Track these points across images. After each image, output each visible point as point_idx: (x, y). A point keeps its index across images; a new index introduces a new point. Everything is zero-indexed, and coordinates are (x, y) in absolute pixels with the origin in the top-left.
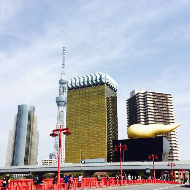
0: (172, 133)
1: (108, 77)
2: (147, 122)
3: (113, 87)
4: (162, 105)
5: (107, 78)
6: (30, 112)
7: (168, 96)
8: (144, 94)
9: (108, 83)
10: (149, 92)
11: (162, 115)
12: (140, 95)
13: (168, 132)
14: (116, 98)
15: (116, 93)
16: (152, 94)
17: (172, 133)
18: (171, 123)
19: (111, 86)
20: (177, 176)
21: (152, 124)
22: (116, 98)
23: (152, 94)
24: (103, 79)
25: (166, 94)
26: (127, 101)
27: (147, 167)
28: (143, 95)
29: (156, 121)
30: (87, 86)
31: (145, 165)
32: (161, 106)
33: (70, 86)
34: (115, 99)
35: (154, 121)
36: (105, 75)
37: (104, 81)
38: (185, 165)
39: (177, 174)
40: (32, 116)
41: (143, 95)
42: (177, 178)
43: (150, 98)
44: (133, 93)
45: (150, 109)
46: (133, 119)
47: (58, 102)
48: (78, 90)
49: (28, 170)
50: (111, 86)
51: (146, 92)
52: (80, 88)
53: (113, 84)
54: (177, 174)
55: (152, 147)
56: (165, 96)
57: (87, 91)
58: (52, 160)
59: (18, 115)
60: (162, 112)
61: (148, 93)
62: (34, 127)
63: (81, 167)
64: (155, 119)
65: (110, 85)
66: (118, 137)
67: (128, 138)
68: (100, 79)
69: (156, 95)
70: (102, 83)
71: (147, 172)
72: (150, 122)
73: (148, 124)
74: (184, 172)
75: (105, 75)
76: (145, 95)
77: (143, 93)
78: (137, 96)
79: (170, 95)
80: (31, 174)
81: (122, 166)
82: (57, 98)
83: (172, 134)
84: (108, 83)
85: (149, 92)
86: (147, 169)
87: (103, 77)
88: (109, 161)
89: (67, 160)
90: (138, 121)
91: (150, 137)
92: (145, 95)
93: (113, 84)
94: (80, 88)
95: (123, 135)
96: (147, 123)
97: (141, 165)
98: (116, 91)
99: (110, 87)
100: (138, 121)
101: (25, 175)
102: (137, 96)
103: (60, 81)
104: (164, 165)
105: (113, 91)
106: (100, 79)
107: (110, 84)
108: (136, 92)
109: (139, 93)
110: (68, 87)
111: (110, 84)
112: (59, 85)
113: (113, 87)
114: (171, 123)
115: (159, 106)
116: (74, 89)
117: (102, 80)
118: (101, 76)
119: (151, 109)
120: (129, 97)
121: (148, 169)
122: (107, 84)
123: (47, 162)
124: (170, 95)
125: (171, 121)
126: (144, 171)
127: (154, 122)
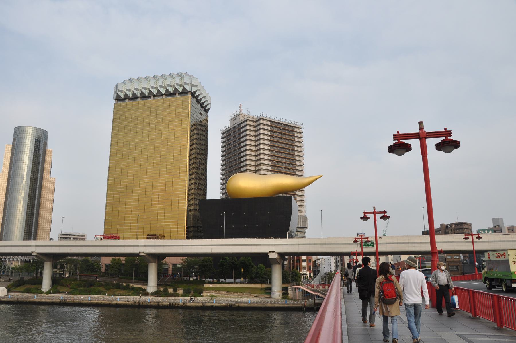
3: (204, 102)
7: (296, 130)
8: (256, 122)
9: (195, 92)
12: (248, 123)
15: (208, 114)
16: (269, 123)
17: (298, 193)
19: (201, 100)
22: (206, 127)
23: (269, 123)
24: (186, 84)
25: (292, 126)
27: (272, 249)
28: (254, 124)
35: (271, 171)
37: (188, 88)
39: (304, 261)
41: (254, 124)
42: (304, 269)
43: (266, 130)
46: (232, 165)
48: (135, 102)
50: (201, 100)
51: (260, 119)
52: (139, 99)
53: (204, 97)
54: (304, 261)
55: (273, 214)
56: (290, 129)
61: (261, 122)
66: (206, 195)
69: (276, 125)
70: (185, 92)
74: (314, 258)
78: (242, 125)
84: (195, 92)
86: (270, 252)
88: (188, 238)
90: (242, 169)
93: (204, 97)
94: (139, 99)
98: (207, 111)
101: (24, 258)
104: (304, 245)
105: (202, 110)
107: (198, 96)
110: (118, 96)
111: (198, 96)
113: (204, 102)
116: (127, 100)
122: (193, 94)
125: (297, 173)
126: (265, 255)
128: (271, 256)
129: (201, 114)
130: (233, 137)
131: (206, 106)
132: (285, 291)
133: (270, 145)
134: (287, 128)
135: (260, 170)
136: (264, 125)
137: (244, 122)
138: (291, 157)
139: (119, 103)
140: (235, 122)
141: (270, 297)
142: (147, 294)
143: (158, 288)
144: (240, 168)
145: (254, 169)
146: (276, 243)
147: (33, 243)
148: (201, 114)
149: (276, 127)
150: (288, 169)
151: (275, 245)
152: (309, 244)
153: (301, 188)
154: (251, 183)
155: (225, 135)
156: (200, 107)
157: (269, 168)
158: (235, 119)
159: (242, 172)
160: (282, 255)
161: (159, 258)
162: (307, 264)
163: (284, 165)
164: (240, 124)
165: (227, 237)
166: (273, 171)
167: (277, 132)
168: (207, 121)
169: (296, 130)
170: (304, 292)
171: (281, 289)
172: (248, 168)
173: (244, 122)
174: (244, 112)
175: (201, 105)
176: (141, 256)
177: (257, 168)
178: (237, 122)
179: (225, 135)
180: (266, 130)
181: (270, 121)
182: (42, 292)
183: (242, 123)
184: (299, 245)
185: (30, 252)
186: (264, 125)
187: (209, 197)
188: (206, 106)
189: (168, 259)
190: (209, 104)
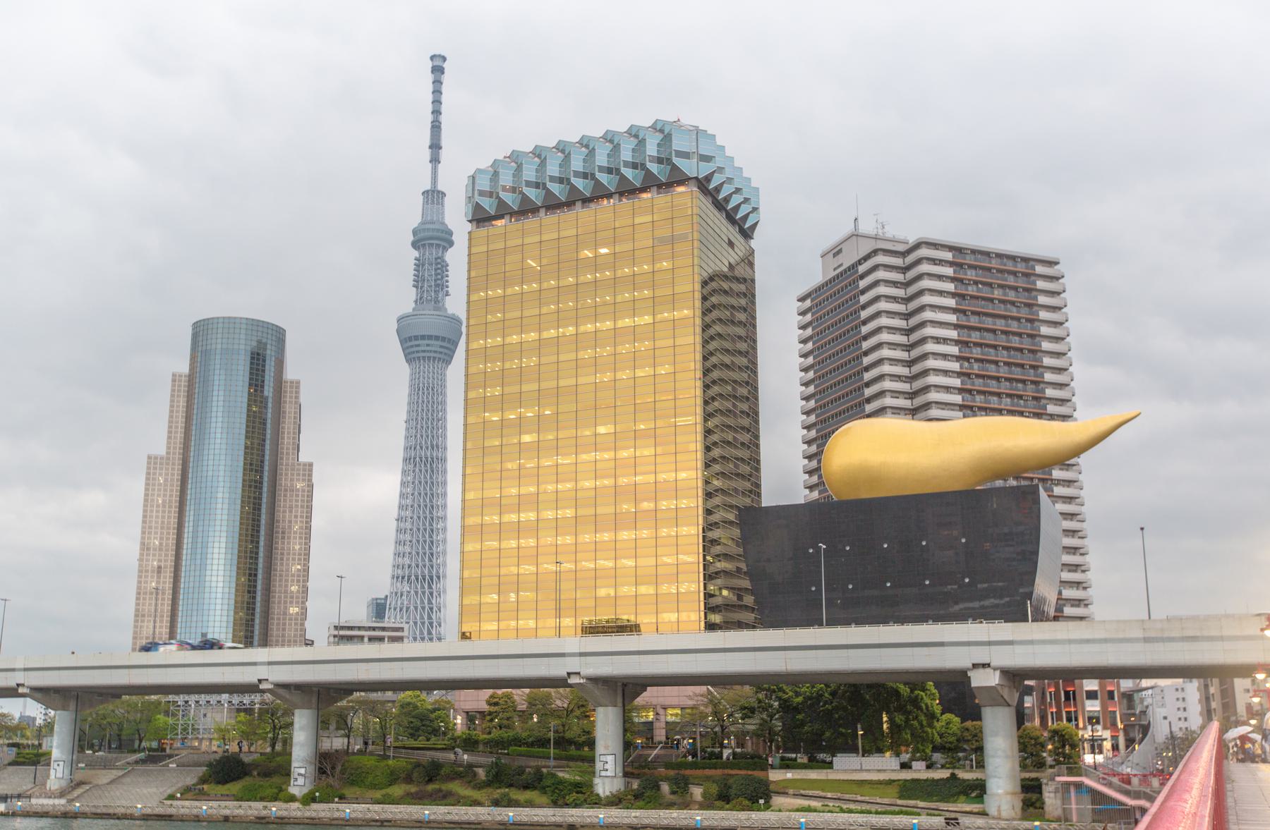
0: (1057, 474)
2: (918, 408)
3: (737, 208)
4: (1000, 321)
7: (1039, 269)
8: (904, 254)
9: (708, 178)
11: (1003, 372)
12: (881, 259)
13: (1026, 471)
15: (753, 243)
16: (948, 256)
17: (1057, 474)
19: (727, 200)
20: (1093, 706)
22: (749, 282)
23: (948, 256)
25: (1026, 260)
26: (802, 299)
27: (980, 655)
28: (898, 261)
29: (971, 408)
32: (1000, 324)
35: (962, 407)
39: (1092, 695)
41: (898, 261)
42: (1093, 720)
44: (840, 251)
45: (938, 340)
47: (410, 339)
48: (530, 222)
50: (727, 200)
51: (917, 246)
52: (542, 211)
53: (738, 190)
54: (1092, 695)
56: (1021, 267)
58: (383, 629)
59: (191, 377)
60: (1003, 356)
61: (924, 252)
62: (286, 440)
63: (563, 655)
64: (967, 396)
65: (721, 197)
66: (759, 495)
69: (969, 260)
71: (974, 684)
74: (1126, 684)
77: (901, 248)
78: (862, 269)
79: (1052, 263)
80: (268, 697)
84: (708, 178)
86: (975, 666)
90: (869, 408)
91: (957, 487)
93: (738, 190)
94: (542, 211)
97: (942, 644)
98: (747, 234)
101: (236, 699)
102: (862, 269)
104: (1088, 641)
107: (718, 189)
110: (478, 208)
111: (718, 189)
112: (416, 254)
113: (737, 208)
115: (989, 323)
117: (676, 160)
119: (945, 341)
120: (816, 276)
121: (985, 666)
122: (702, 184)
123: (362, 637)
125: (1051, 409)
128: (980, 680)
129: (731, 244)
130: (836, 309)
131: (746, 217)
132: (1031, 794)
133: (956, 327)
134: (1010, 266)
135: (927, 406)
137: (866, 258)
138: (1027, 360)
139: (483, 232)
140: (840, 259)
141: (984, 814)
142: (597, 802)
143: (627, 784)
144: (861, 404)
145: (906, 403)
146: (993, 638)
147: (259, 654)
148: (731, 244)
149: (971, 267)
150: (1020, 397)
151: (990, 643)
152: (1105, 641)
153: (1066, 458)
154: (897, 448)
155: (808, 303)
156: (725, 222)
157: (957, 399)
158: (837, 251)
159: (869, 416)
160: (1014, 676)
161: (626, 690)
162: (1104, 706)
163: (1005, 387)
164: (854, 267)
165: (832, 622)
166: (968, 410)
167: (976, 283)
168: (751, 265)
169: (1039, 269)
170: (1097, 797)
171: (1019, 789)
172: (888, 401)
173: (866, 258)
174: (867, 227)
175: (730, 218)
176: (570, 686)
177: (919, 401)
178: (847, 260)
179: (808, 303)
180: (940, 277)
181: (951, 248)
182: (292, 799)
183: (860, 262)
185: (255, 680)
187: (768, 499)
188: (746, 217)
189: (651, 695)
190: (755, 209)
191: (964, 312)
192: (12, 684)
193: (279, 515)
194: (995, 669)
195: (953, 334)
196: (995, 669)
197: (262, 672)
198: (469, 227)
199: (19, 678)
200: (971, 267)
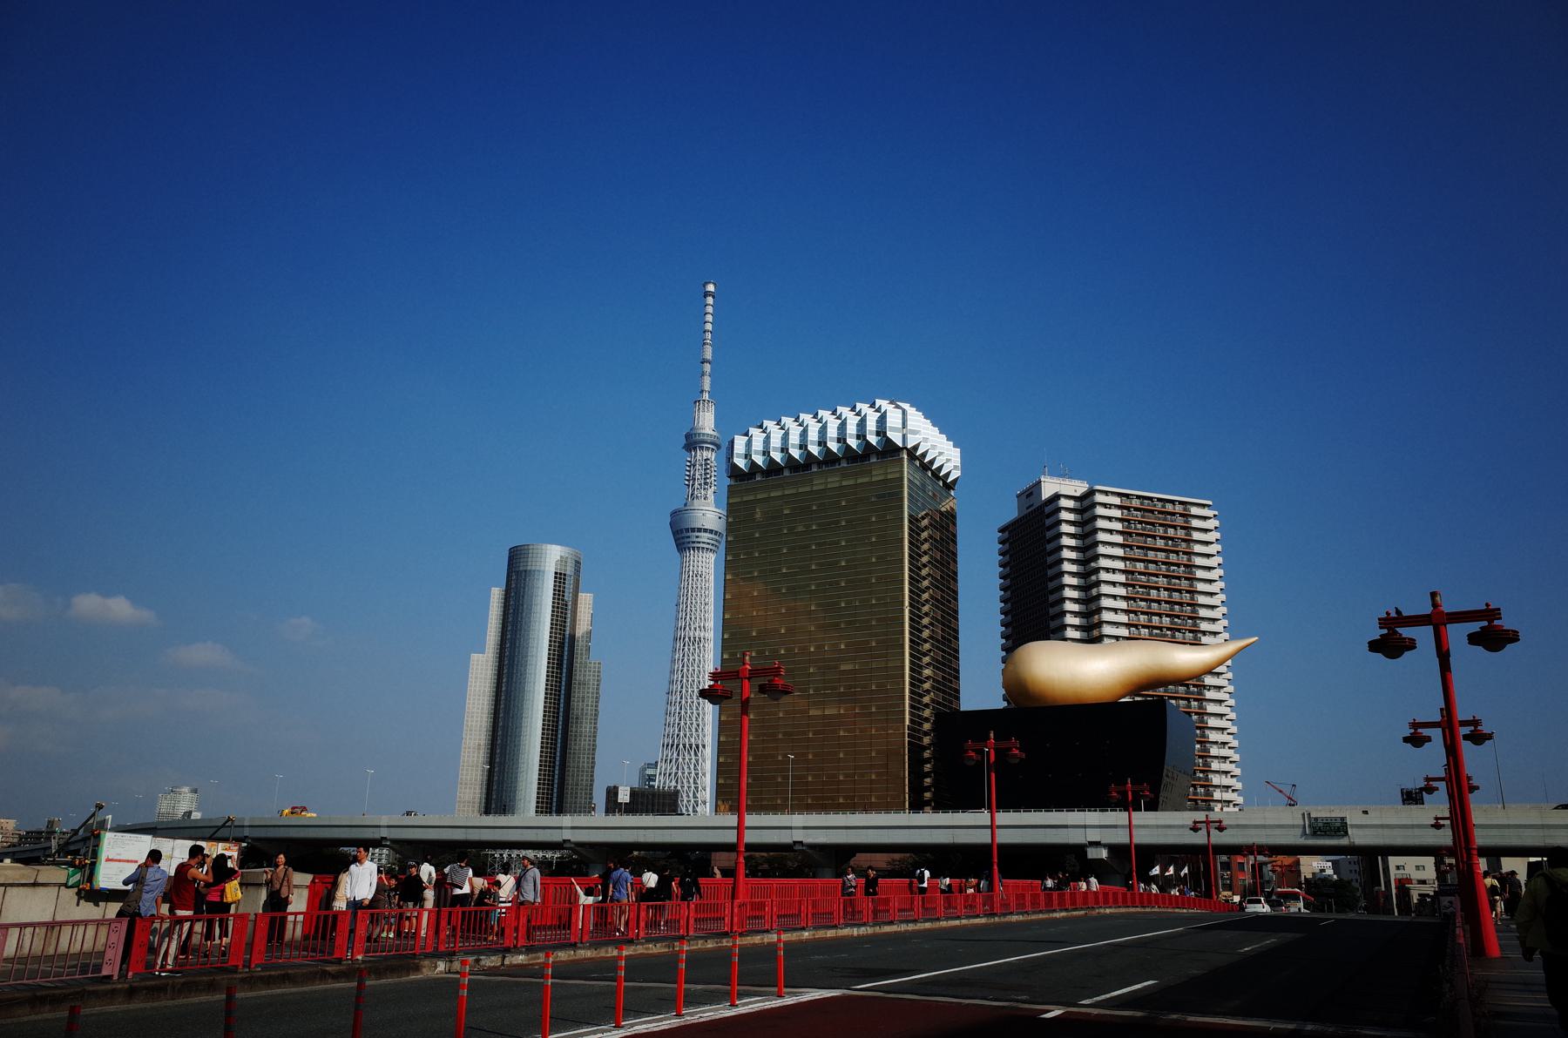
0: (1209, 680)
1: (916, 419)
3: (941, 467)
5: (911, 425)
6: (560, 577)
7: (1194, 511)
9: (916, 448)
10: (1106, 493)
14: (951, 516)
16: (1116, 501)
17: (1209, 680)
18: (1204, 633)
19: (932, 462)
21: (1117, 638)
22: (954, 517)
23: (1116, 501)
24: (894, 429)
25: (1181, 503)
26: (1001, 531)
27: (1093, 836)
30: (820, 463)
31: (1085, 827)
33: (741, 463)
34: (946, 522)
35: (1128, 625)
36: (904, 412)
37: (896, 438)
38: (1264, 826)
40: (568, 597)
45: (1107, 570)
49: (555, 837)
50: (932, 462)
51: (1091, 493)
52: (787, 473)
56: (1179, 509)
57: (818, 484)
61: (1099, 498)
66: (958, 698)
67: (1002, 705)
68: (881, 432)
69: (1136, 503)
70: (890, 450)
72: (1107, 630)
73: (1098, 640)
75: (904, 412)
76: (1086, 503)
78: (1047, 510)
81: (998, 831)
82: (675, 514)
83: (1210, 687)
84: (916, 448)
85: (1106, 493)
87: (894, 419)
88: (917, 806)
89: (727, 796)
90: (1053, 625)
92: (1086, 503)
94: (787, 473)
95: (980, 690)
96: (1095, 633)
97: (1066, 827)
99: (926, 467)
100: (1053, 625)
101: (540, 854)
103: (688, 436)
104: (1170, 827)
106: (881, 432)
107: (924, 455)
108: (1047, 491)
109: (1057, 497)
110: (735, 466)
111: (924, 455)
113: (941, 467)
114: (1204, 633)
117: (889, 434)
118: (882, 420)
119: (1114, 571)
120: (1010, 513)
121: (1097, 844)
122: (912, 452)
124: (1204, 506)
126: (1079, 850)
127: (1124, 632)
128: (1092, 853)
131: (948, 474)
133: (1123, 559)
136: (1105, 505)
147: (566, 820)
169: (1194, 511)
181: (1119, 495)
184: (1158, 827)
186: (1105, 505)
191: (1131, 547)
192: (377, 836)
193: (574, 703)
194: (1105, 846)
195: (1120, 565)
196: (1105, 846)
197: (567, 835)
198: (728, 481)
199: (384, 833)
200: (1136, 509)
